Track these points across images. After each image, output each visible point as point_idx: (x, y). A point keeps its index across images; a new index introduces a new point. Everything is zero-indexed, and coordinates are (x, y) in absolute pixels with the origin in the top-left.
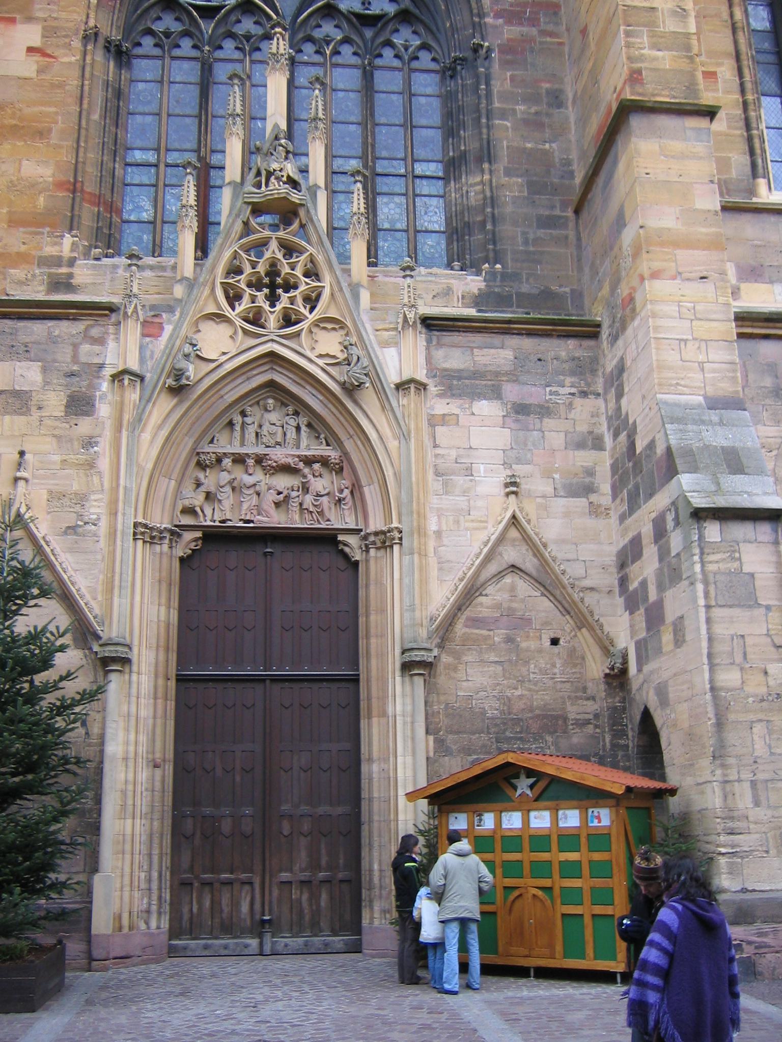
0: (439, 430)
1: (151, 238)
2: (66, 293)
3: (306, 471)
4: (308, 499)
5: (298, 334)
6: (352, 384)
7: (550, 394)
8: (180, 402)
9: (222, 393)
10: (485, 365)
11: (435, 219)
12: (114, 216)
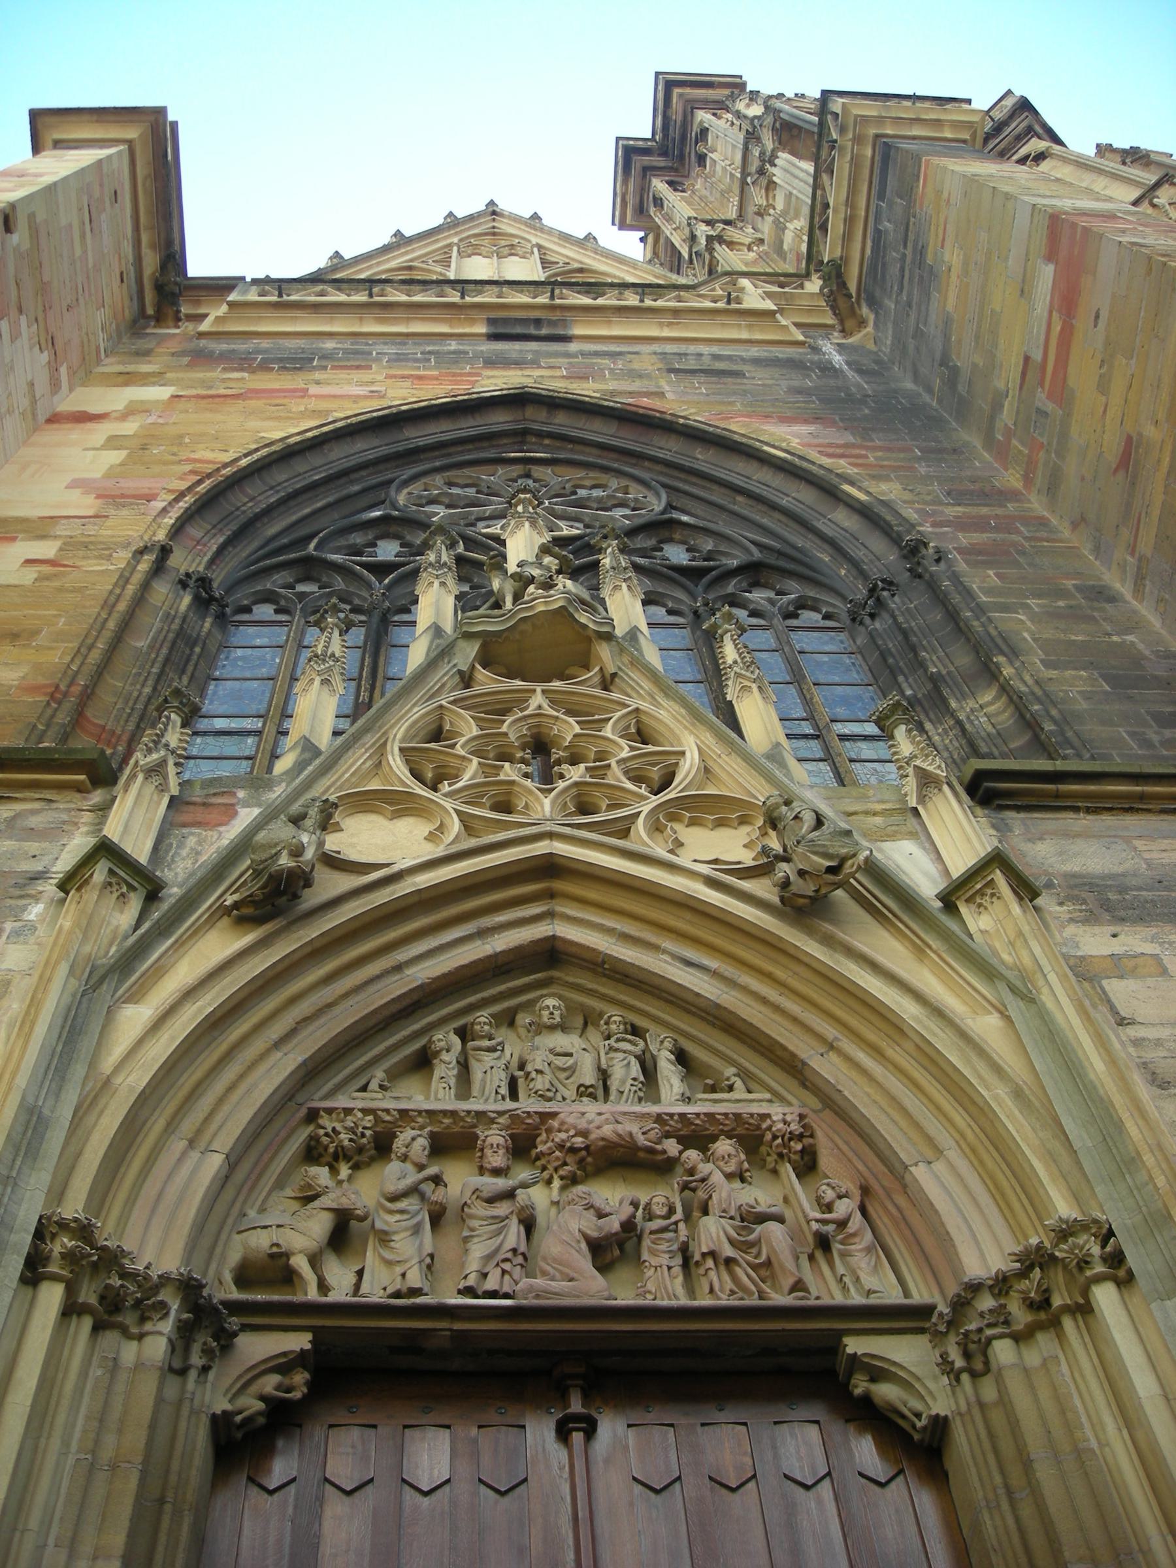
3: (692, 1155)
9: (402, 955)
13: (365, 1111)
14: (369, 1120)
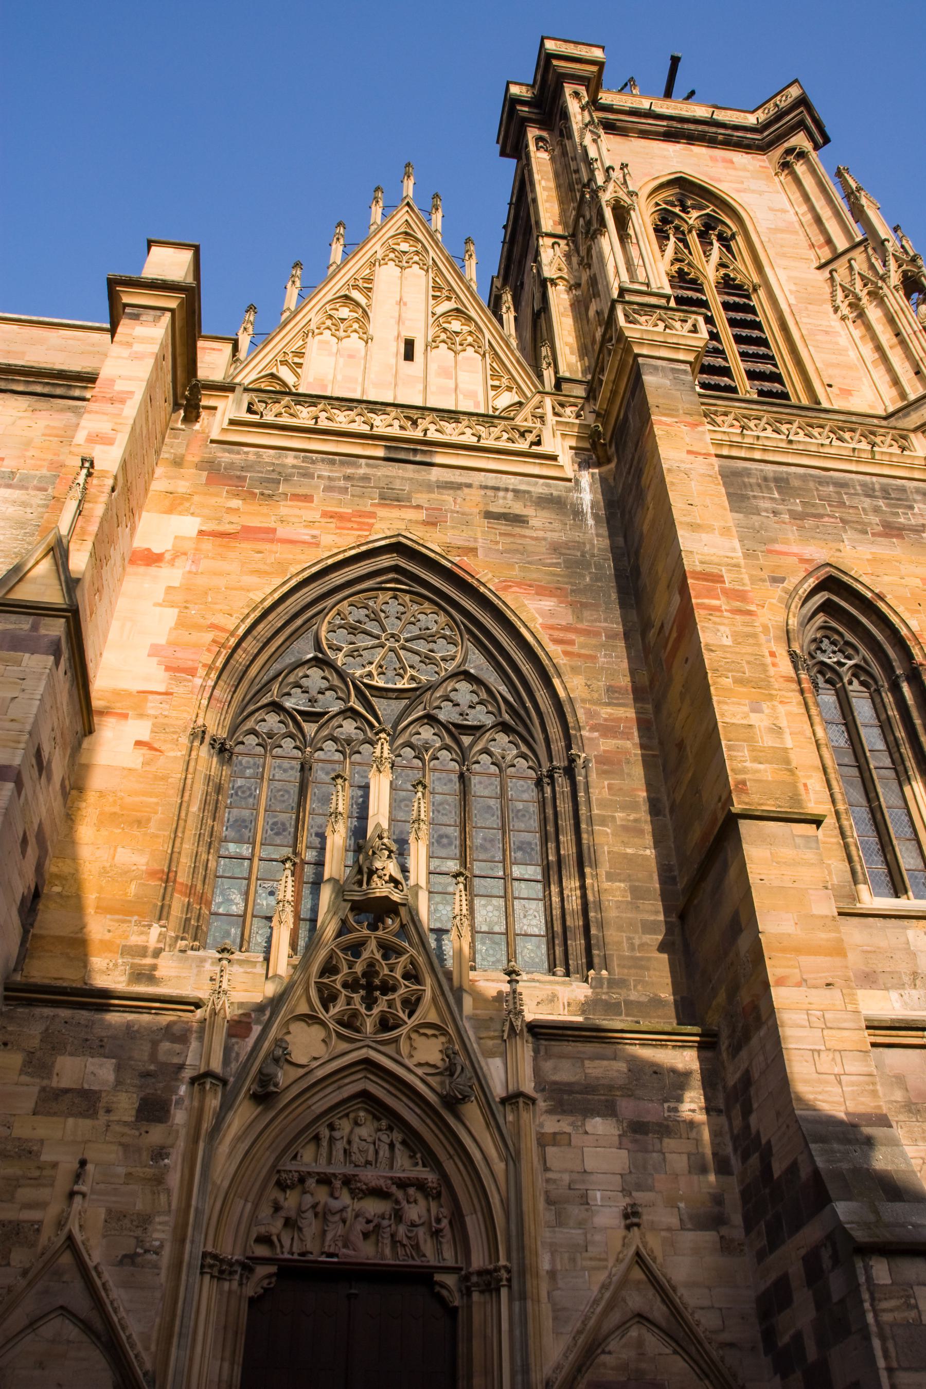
0: (551, 1151)
1: (239, 933)
2: (148, 986)
3: (399, 1194)
4: (402, 1230)
5: (396, 1040)
6: (456, 1097)
7: (669, 1111)
8: (265, 1110)
9: (310, 1102)
10: (597, 1078)
11: (534, 922)
12: (203, 908)
13: (296, 1171)
14: (296, 1175)
